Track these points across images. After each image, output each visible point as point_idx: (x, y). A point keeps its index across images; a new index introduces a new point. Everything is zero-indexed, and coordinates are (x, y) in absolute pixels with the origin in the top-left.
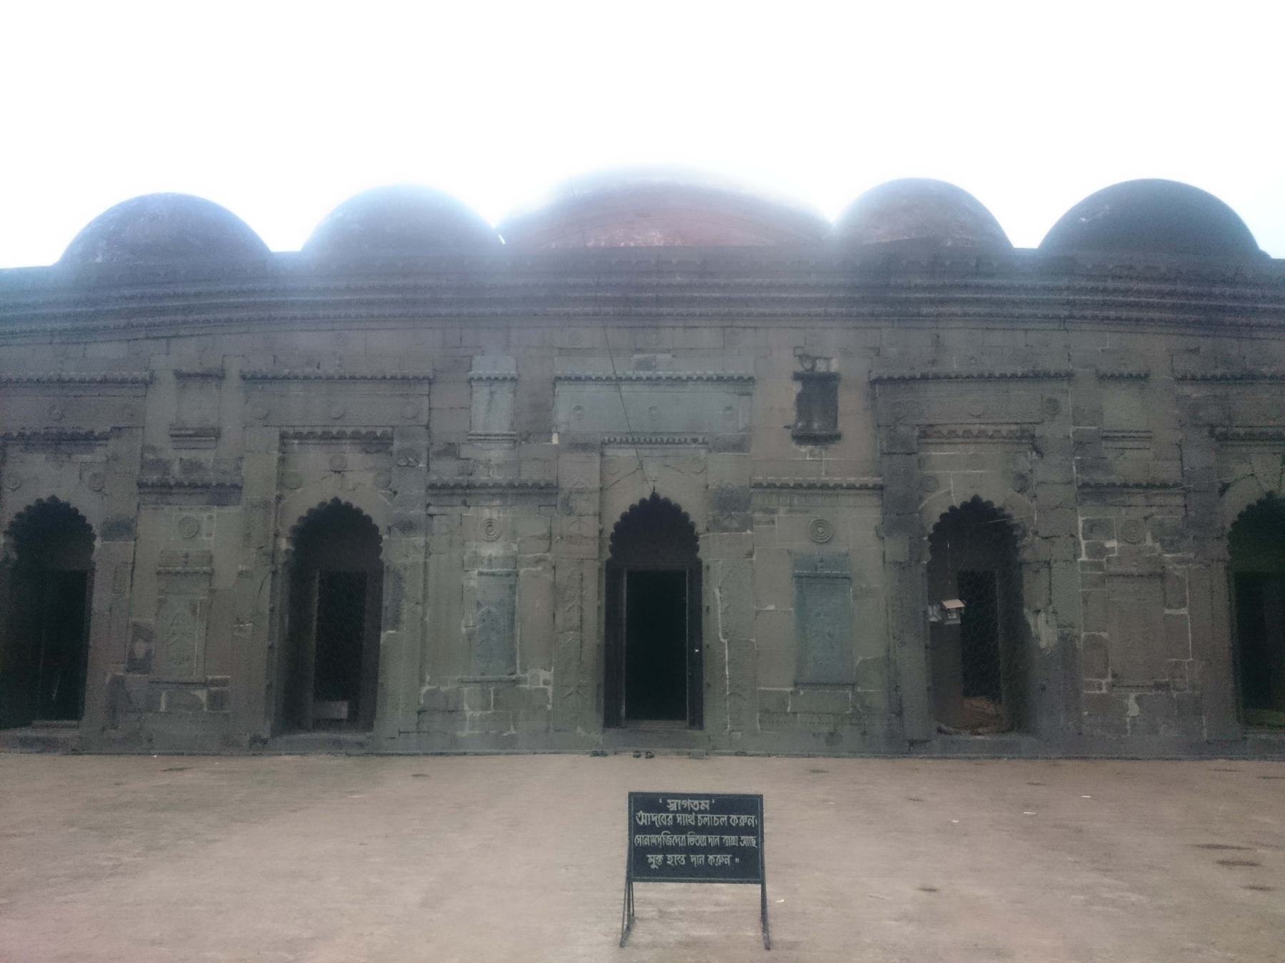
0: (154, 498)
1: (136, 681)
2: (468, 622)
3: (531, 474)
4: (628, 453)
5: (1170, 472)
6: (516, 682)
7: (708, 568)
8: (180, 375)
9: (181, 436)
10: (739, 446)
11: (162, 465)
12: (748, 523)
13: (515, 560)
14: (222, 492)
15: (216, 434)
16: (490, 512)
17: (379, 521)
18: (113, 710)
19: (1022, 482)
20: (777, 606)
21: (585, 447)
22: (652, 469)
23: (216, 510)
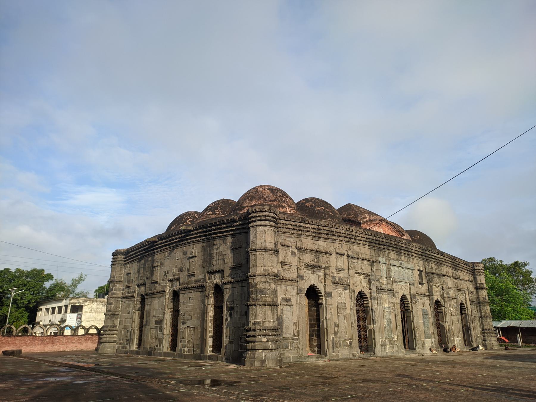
0: (334, 286)
1: (336, 338)
2: (385, 324)
3: (390, 287)
4: (399, 283)
5: (454, 295)
6: (393, 338)
7: (412, 312)
8: (337, 253)
9: (337, 269)
10: (413, 284)
11: (334, 277)
12: (416, 302)
13: (389, 308)
14: (346, 286)
15: (343, 270)
16: (385, 296)
17: (368, 296)
18: (333, 347)
19: (442, 295)
20: (421, 321)
21: (396, 282)
22: (403, 287)
23: (345, 291)
